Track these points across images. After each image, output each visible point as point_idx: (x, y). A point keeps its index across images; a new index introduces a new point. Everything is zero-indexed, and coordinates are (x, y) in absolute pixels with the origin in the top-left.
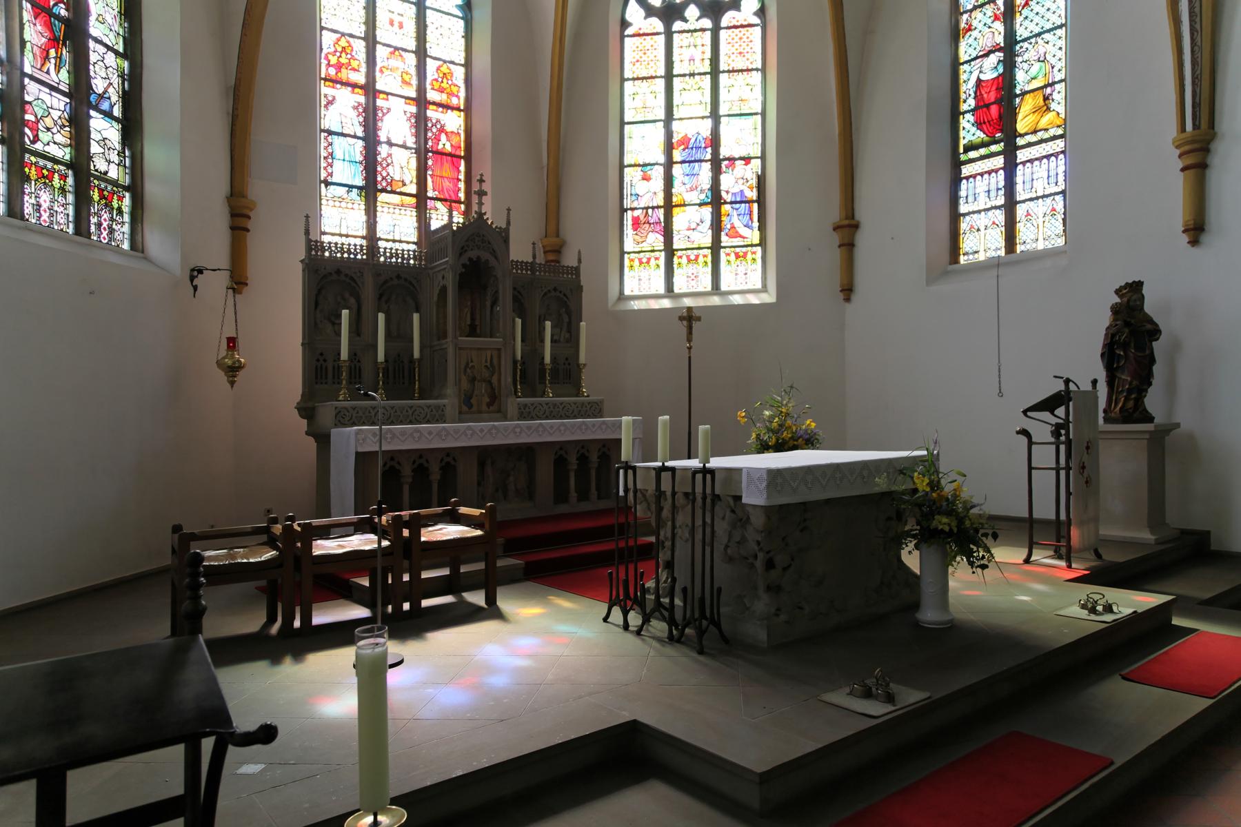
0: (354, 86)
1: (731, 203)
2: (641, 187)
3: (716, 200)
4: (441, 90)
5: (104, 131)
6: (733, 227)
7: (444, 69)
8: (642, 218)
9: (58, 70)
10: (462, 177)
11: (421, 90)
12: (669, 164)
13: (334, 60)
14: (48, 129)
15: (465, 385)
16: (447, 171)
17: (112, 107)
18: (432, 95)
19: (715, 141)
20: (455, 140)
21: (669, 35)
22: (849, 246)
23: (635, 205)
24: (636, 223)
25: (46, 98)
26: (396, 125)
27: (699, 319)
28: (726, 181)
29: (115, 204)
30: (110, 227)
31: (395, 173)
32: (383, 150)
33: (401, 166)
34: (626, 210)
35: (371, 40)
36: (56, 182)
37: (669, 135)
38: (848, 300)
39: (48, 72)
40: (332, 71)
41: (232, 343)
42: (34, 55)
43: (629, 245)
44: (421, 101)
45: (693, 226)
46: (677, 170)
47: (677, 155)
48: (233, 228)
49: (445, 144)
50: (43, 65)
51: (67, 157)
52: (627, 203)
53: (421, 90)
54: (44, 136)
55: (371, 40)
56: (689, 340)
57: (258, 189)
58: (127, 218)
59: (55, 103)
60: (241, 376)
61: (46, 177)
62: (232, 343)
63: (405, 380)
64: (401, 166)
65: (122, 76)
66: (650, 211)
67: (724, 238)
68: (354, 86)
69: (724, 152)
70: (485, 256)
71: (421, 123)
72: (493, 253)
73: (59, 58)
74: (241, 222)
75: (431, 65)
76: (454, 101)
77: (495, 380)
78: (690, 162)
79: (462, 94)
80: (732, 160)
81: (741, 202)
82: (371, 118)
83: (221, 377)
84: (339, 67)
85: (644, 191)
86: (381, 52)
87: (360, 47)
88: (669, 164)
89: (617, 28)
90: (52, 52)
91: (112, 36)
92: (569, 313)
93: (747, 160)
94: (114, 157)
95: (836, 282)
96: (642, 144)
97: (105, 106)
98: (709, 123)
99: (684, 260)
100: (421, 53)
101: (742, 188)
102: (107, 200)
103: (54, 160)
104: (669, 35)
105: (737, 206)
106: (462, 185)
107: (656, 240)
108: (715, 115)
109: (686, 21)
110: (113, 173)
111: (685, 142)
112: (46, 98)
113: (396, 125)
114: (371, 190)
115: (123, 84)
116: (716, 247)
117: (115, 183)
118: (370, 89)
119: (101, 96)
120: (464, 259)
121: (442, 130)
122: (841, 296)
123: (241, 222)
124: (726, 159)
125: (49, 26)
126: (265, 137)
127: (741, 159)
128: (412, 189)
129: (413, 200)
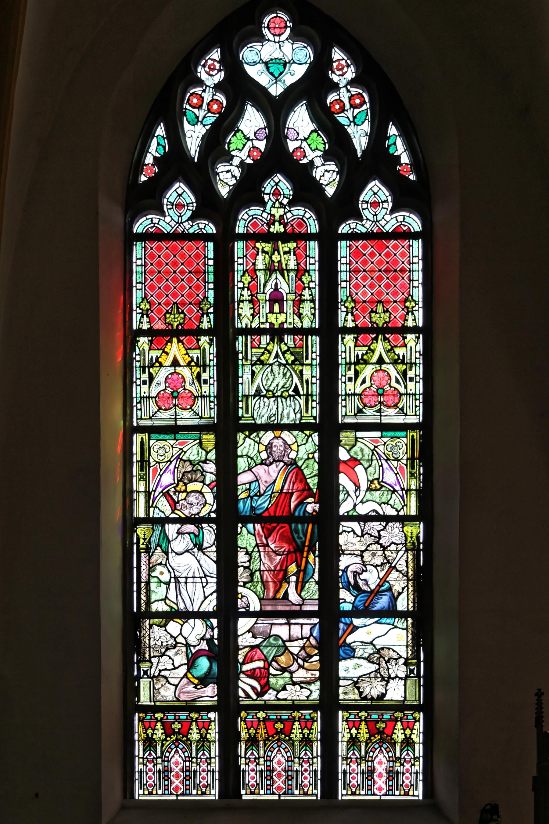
9: (300, 587)
14: (284, 670)
17: (394, 599)
25: (282, 631)
29: (399, 735)
30: (389, 772)
36: (297, 732)
39: (286, 596)
42: (265, 584)
50: (277, 591)
51: (315, 695)
54: (277, 681)
58: (419, 750)
59: (296, 631)
61: (282, 731)
65: (415, 549)
90: (293, 568)
91: (396, 500)
97: (383, 602)
103: (295, 706)
110: (396, 692)
112: (282, 631)
115: (416, 558)
117: (400, 706)
119: (377, 593)
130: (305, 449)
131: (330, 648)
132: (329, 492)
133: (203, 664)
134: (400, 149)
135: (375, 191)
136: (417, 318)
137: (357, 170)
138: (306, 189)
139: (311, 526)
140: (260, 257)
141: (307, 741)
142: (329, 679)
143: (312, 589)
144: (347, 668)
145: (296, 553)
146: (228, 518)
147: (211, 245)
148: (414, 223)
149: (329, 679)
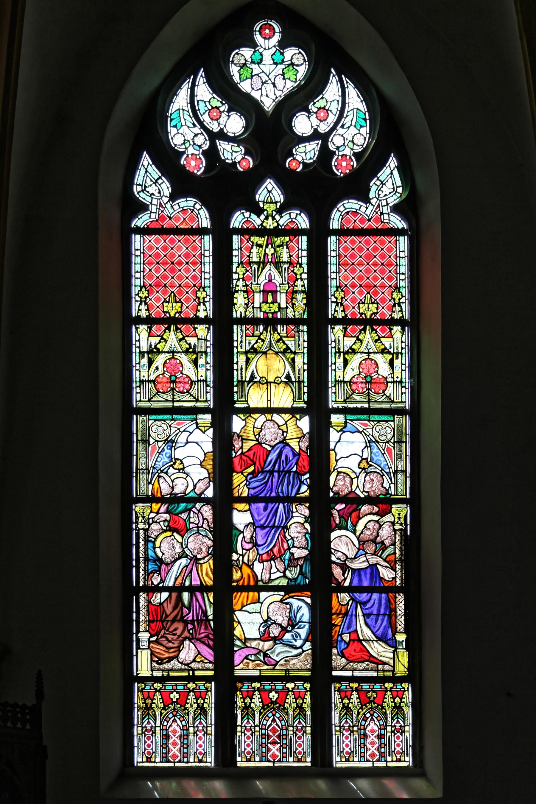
1: (350, 590)
2: (167, 546)
3: (318, 578)
6: (356, 640)
8: (169, 608)
23: (156, 580)
28: (342, 543)
34: (138, 590)
43: (143, 664)
45: (275, 631)
66: (186, 596)
67: (337, 661)
69: (337, 484)
78: (267, 500)
80: (353, 501)
81: (370, 590)
85: (176, 553)
93: (383, 503)
101: (373, 559)
105: (364, 597)
109: (259, 211)
116: (321, 677)
124: (339, 499)
127: (370, 500)
140: (255, 250)
147: (304, 238)
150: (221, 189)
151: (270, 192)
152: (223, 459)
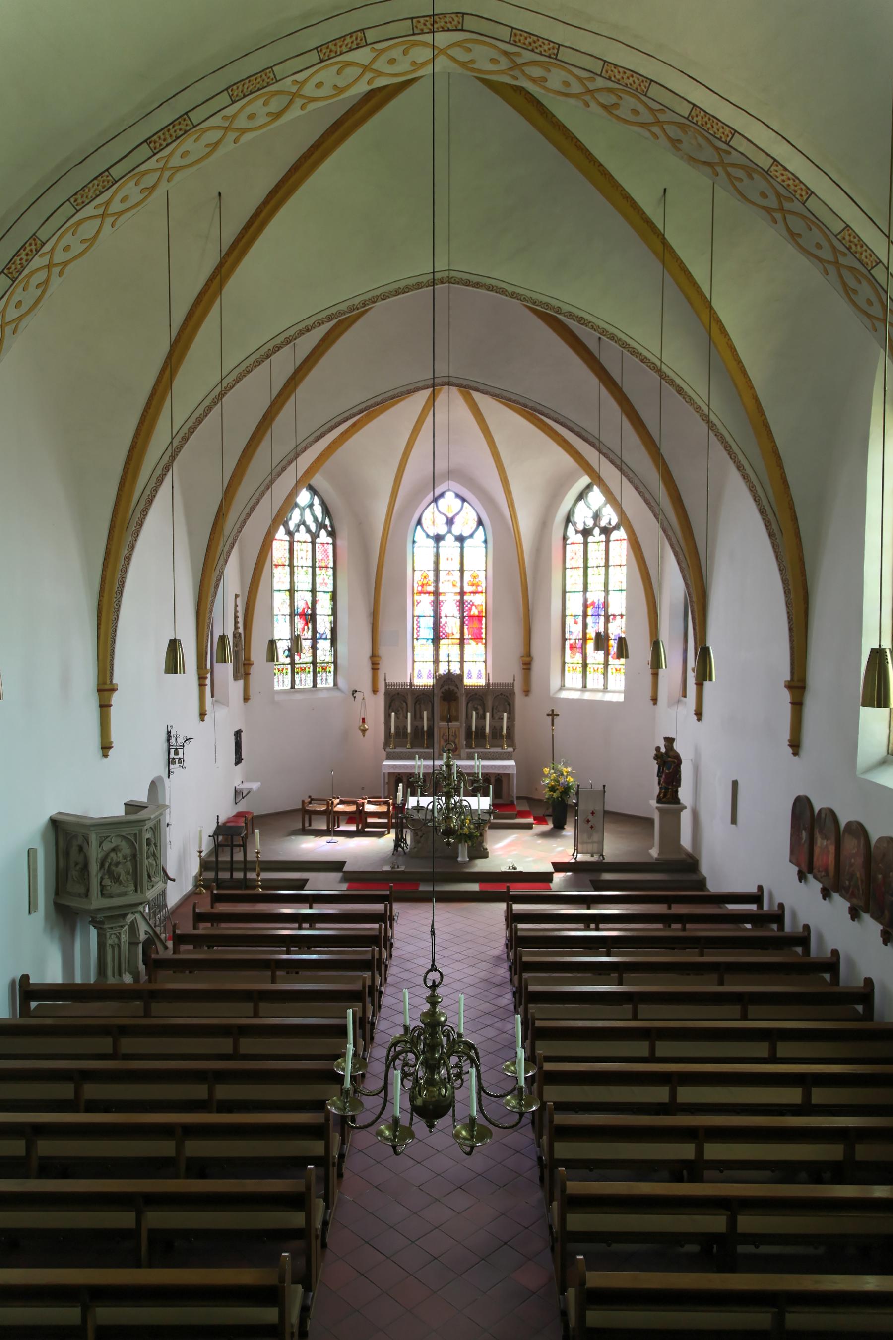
0: (429, 593)
4: (473, 585)
5: (324, 646)
7: (475, 575)
10: (484, 626)
11: (462, 588)
12: (585, 615)
13: (420, 584)
15: (443, 743)
16: (476, 625)
18: (467, 589)
19: (606, 605)
20: (480, 608)
21: (586, 544)
22: (655, 675)
24: (571, 647)
26: (450, 608)
27: (557, 715)
31: (448, 629)
32: (443, 620)
33: (452, 625)
35: (436, 570)
36: (307, 670)
37: (585, 601)
38: (655, 704)
40: (420, 589)
41: (364, 720)
43: (568, 659)
44: (462, 593)
46: (590, 620)
47: (590, 611)
48: (373, 669)
49: (474, 612)
52: (567, 636)
53: (462, 588)
55: (436, 570)
56: (553, 725)
57: (383, 651)
60: (367, 733)
62: (364, 720)
63: (421, 740)
64: (452, 625)
68: (429, 593)
70: (452, 687)
71: (462, 604)
72: (457, 686)
73: (308, 628)
74: (376, 667)
75: (467, 576)
76: (480, 589)
77: (457, 741)
79: (484, 585)
82: (436, 605)
83: (360, 733)
84: (422, 586)
86: (442, 575)
87: (431, 575)
88: (585, 615)
89: (561, 543)
92: (509, 705)
93: (622, 616)
94: (328, 653)
95: (648, 693)
96: (574, 605)
97: (324, 636)
98: (603, 594)
99: (592, 670)
100: (462, 571)
102: (324, 669)
104: (586, 544)
106: (483, 631)
107: (578, 657)
108: (607, 591)
111: (593, 604)
113: (450, 608)
114: (436, 640)
118: (436, 593)
120: (443, 690)
121: (473, 605)
122: (652, 702)
123: (376, 667)
125: (305, 620)
126: (386, 627)
128: (458, 636)
129: (458, 641)
130: (308, 597)
131: (314, 648)
132: (314, 608)
133: (287, 652)
134: (327, 522)
135: (323, 533)
136: (331, 565)
137: (321, 526)
138: (308, 531)
139: (311, 618)
141: (309, 672)
142: (314, 655)
143: (310, 633)
144: (319, 653)
145: (306, 624)
146: (292, 615)
148: (330, 540)
149: (314, 655)
150: (586, 533)
151: (597, 531)
152: (586, 606)
